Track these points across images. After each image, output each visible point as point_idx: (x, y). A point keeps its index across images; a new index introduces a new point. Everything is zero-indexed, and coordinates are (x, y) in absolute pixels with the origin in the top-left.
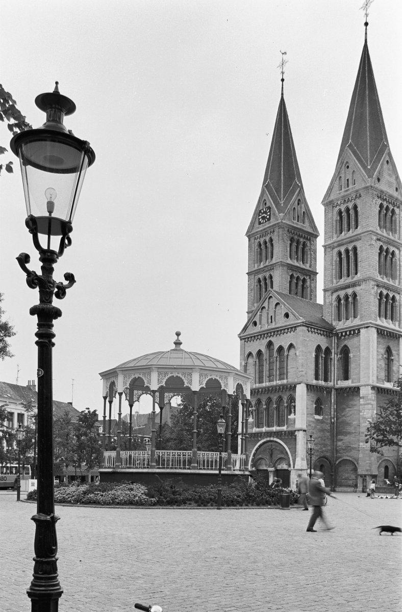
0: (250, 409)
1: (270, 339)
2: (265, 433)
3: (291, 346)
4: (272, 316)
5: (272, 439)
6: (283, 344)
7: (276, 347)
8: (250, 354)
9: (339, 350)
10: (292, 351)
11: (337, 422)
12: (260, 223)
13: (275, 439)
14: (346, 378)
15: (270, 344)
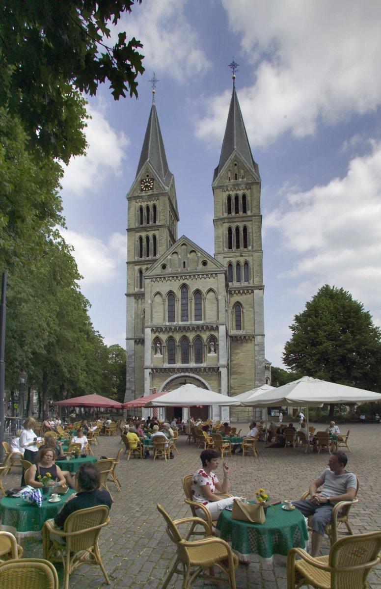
0: (158, 345)
1: (184, 282)
2: (178, 368)
3: (211, 290)
4: (184, 263)
5: (187, 374)
6: (200, 288)
7: (192, 289)
8: (158, 293)
9: (232, 305)
10: (211, 294)
11: (231, 364)
12: (142, 190)
13: (191, 375)
14: (239, 326)
15: (184, 287)
